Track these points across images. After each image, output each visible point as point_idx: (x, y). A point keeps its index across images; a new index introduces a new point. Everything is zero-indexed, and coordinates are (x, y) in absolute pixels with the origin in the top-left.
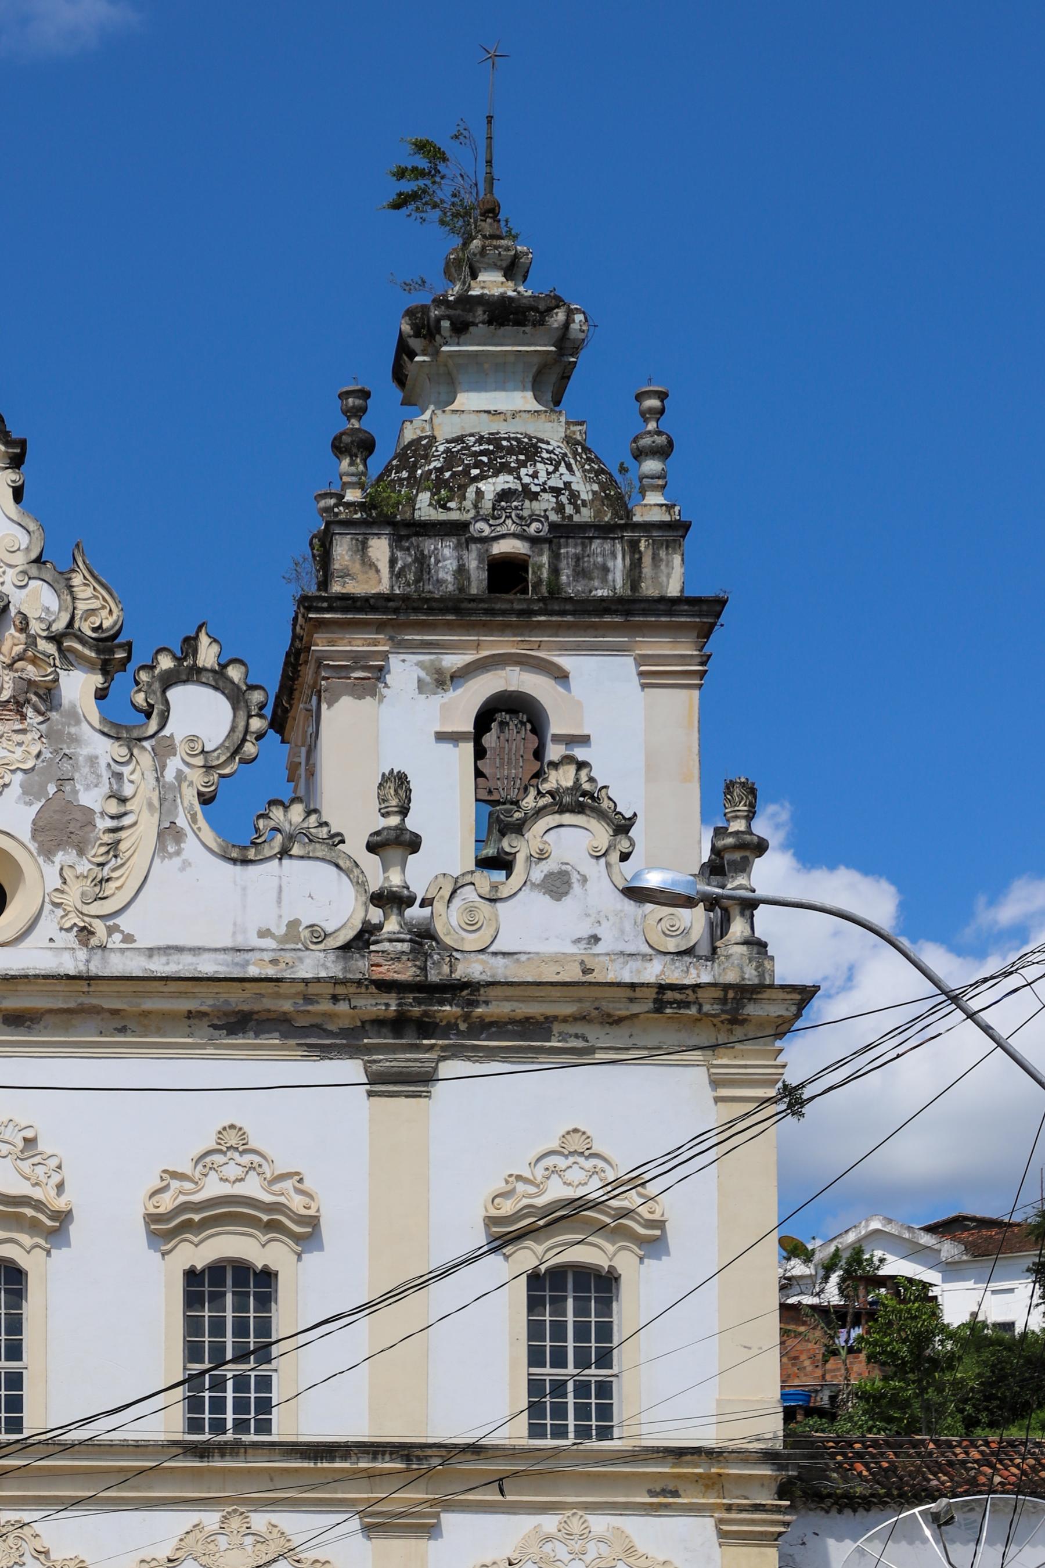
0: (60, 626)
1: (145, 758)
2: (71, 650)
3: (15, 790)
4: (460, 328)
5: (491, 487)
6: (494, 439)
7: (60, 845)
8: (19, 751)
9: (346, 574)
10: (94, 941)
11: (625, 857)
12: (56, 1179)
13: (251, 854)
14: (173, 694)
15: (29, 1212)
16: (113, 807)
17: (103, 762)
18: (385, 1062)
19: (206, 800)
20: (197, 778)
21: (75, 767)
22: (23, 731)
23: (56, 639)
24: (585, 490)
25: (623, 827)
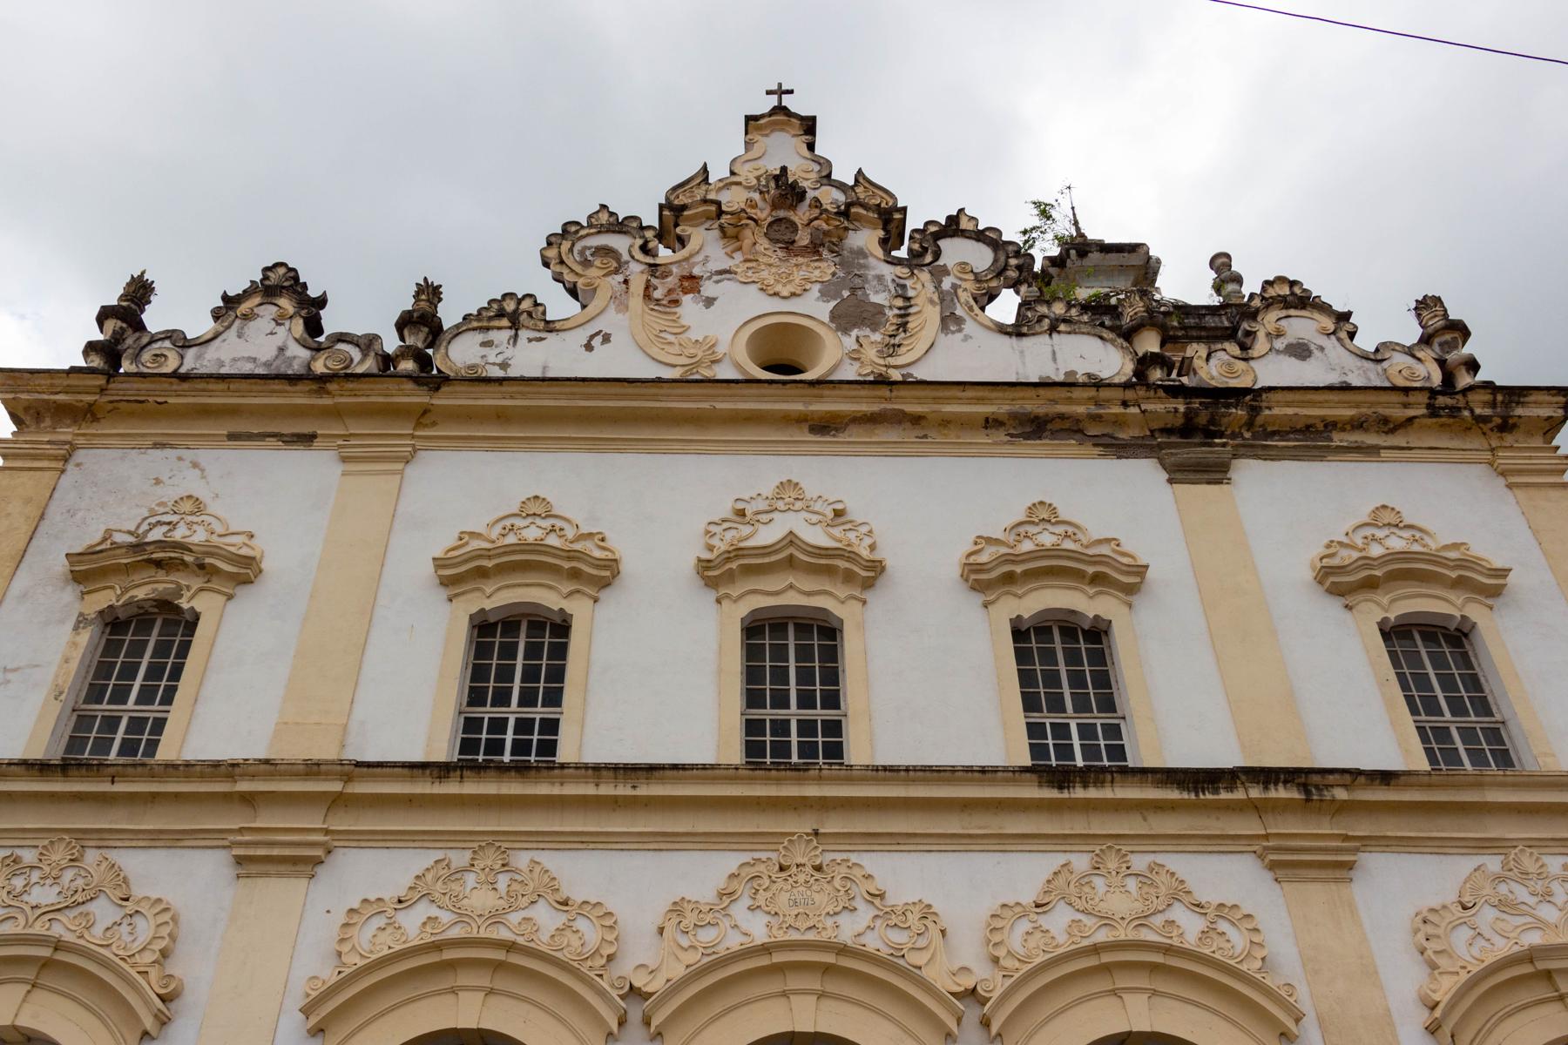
2: (858, 218)
7: (855, 325)
8: (817, 273)
11: (1352, 335)
12: (868, 541)
13: (1025, 330)
14: (943, 243)
15: (842, 564)
16: (900, 302)
17: (889, 278)
20: (971, 286)
21: (866, 281)
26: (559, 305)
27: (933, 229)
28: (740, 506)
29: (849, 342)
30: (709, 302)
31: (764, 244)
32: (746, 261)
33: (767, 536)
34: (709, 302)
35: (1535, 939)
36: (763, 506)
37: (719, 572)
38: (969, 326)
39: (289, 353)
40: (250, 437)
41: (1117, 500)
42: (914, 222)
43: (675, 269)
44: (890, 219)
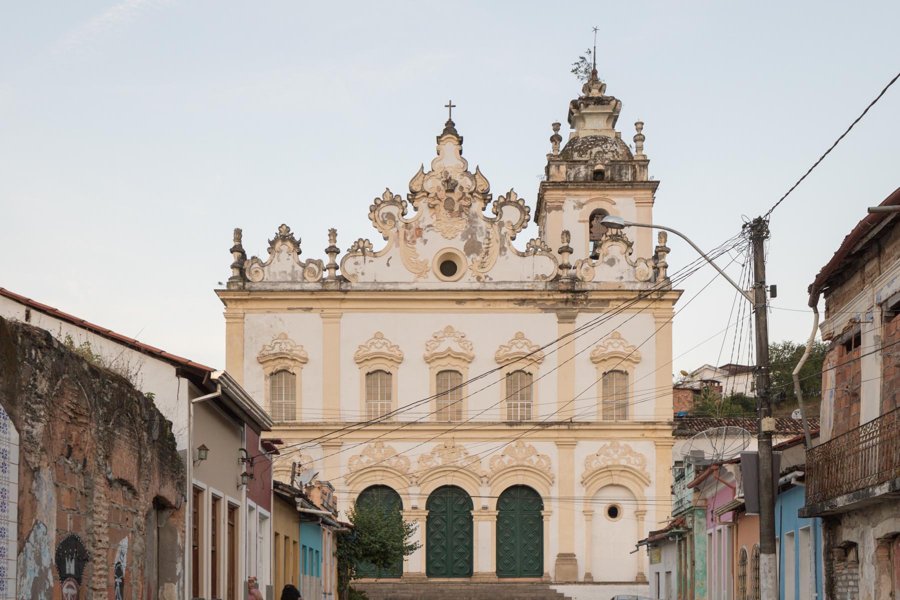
0: (472, 190)
1: (496, 227)
4: (587, 106)
5: (595, 150)
6: (595, 137)
9: (553, 175)
11: (630, 254)
16: (487, 241)
17: (484, 228)
18: (563, 313)
23: (471, 193)
24: (620, 151)
25: (630, 245)
26: (378, 244)
27: (502, 200)
29: (469, 260)
30: (425, 241)
31: (442, 209)
33: (442, 348)
36: (441, 335)
37: (428, 360)
38: (508, 252)
39: (296, 269)
40: (294, 309)
41: (541, 326)
42: (495, 198)
43: (413, 224)
44: (486, 197)
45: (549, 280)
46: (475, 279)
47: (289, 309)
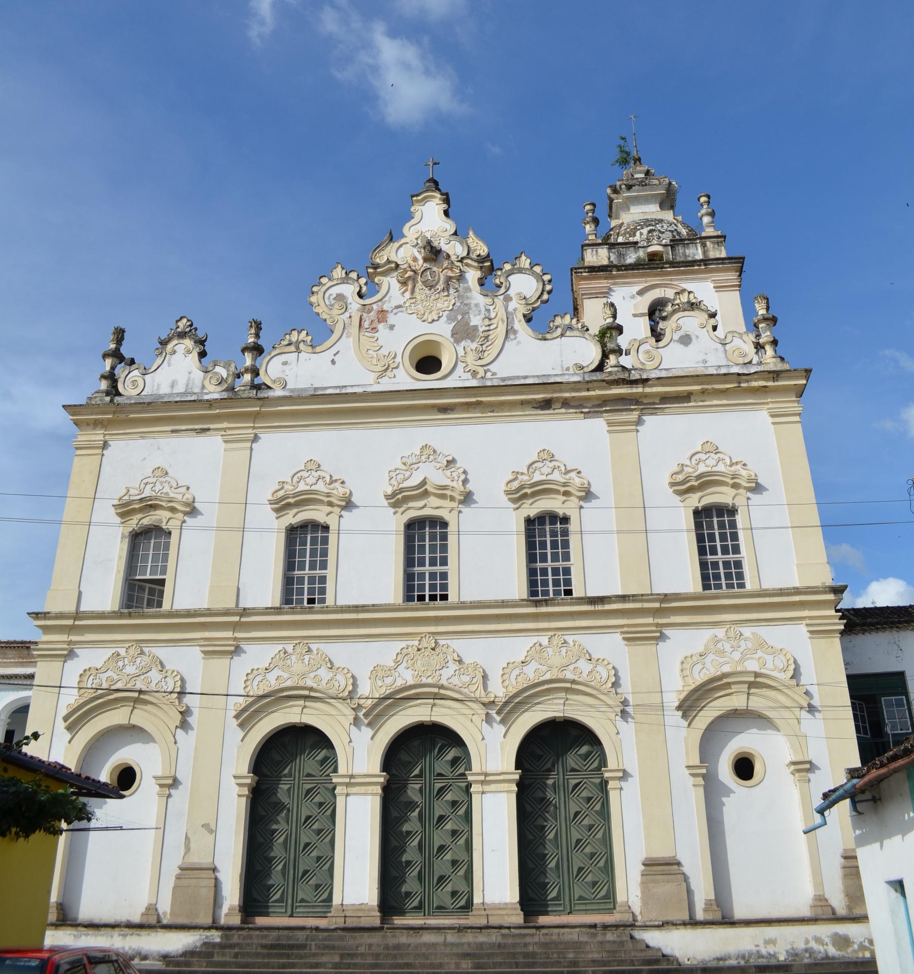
1: (499, 301)
3: (444, 319)
7: (462, 340)
10: (479, 376)
14: (510, 278)
16: (487, 322)
19: (528, 319)
21: (470, 308)
22: (448, 296)
28: (404, 460)
30: (392, 327)
32: (411, 298)
34: (392, 327)
35: (726, 669)
41: (579, 442)
45: (586, 370)
46: (469, 375)
47: (173, 431)
